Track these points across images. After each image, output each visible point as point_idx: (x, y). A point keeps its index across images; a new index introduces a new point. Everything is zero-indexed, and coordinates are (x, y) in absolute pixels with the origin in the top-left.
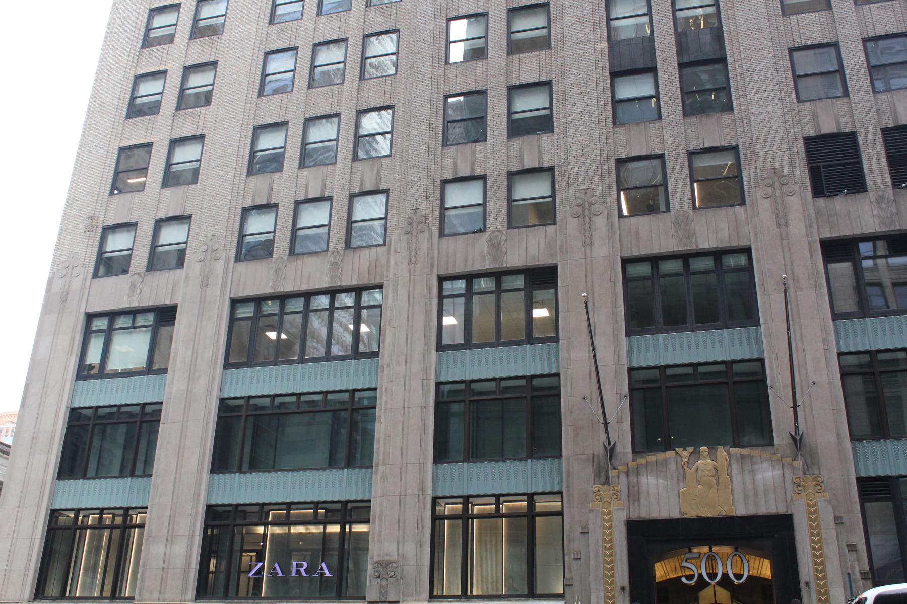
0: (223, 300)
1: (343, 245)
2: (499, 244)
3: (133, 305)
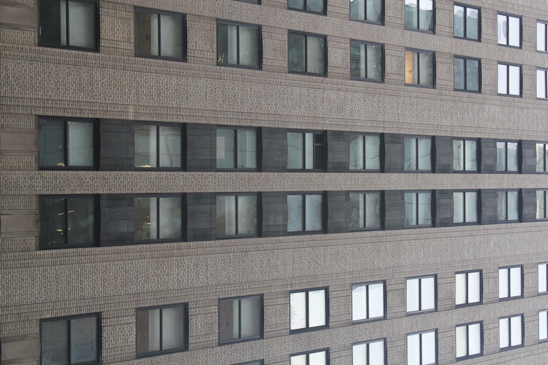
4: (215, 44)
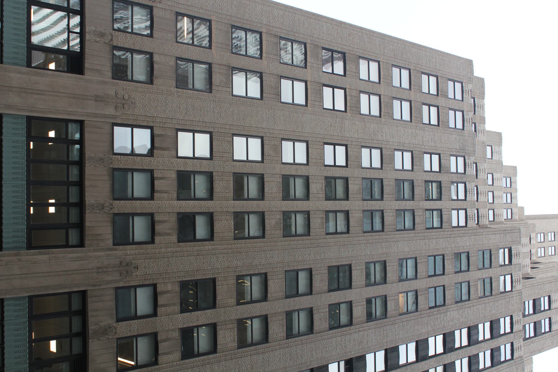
0: (83, 116)
1: (117, 212)
2: (106, 334)
3: (87, 34)
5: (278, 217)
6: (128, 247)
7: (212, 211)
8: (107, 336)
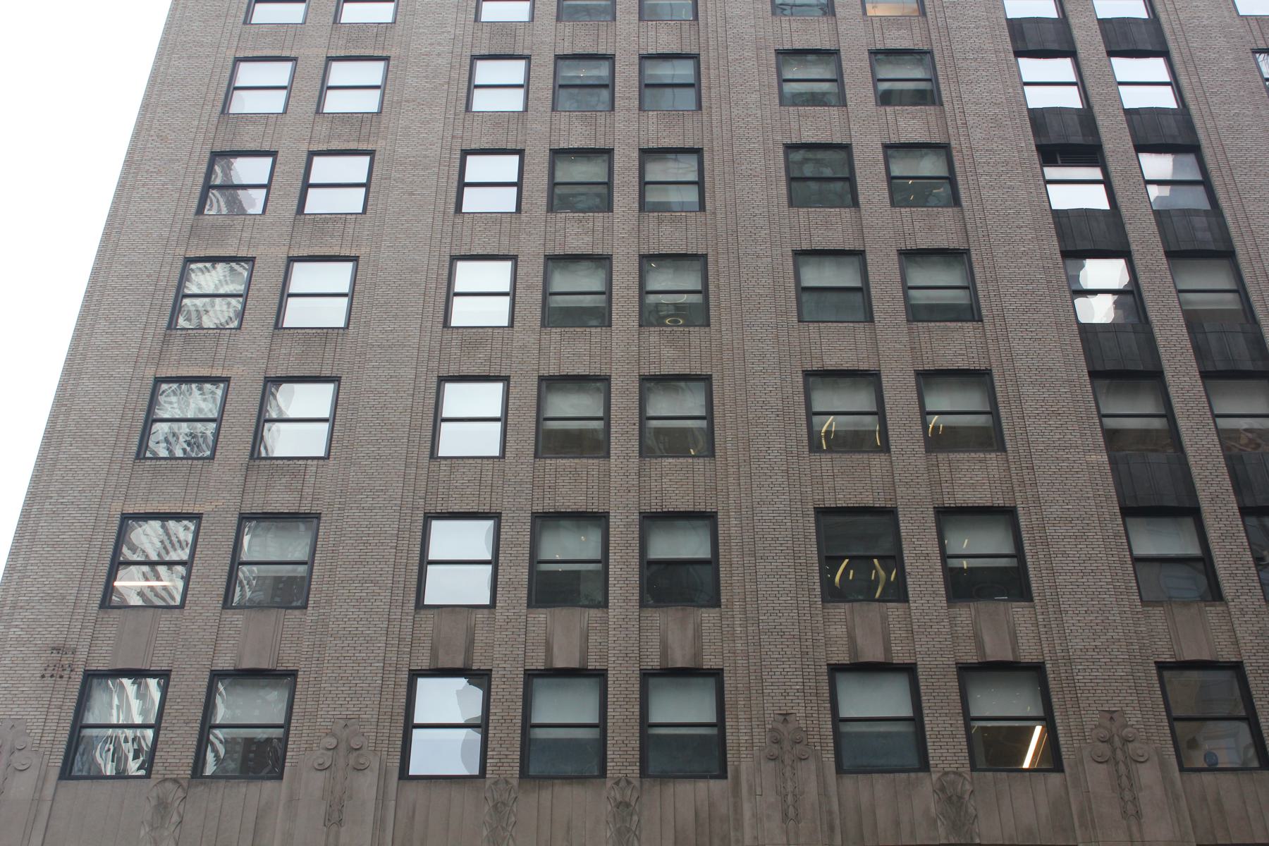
1: (637, 768)
2: (960, 798)
4: (949, 324)
5: (654, 339)
6: (729, 738)
7: (636, 517)
8: (967, 796)
